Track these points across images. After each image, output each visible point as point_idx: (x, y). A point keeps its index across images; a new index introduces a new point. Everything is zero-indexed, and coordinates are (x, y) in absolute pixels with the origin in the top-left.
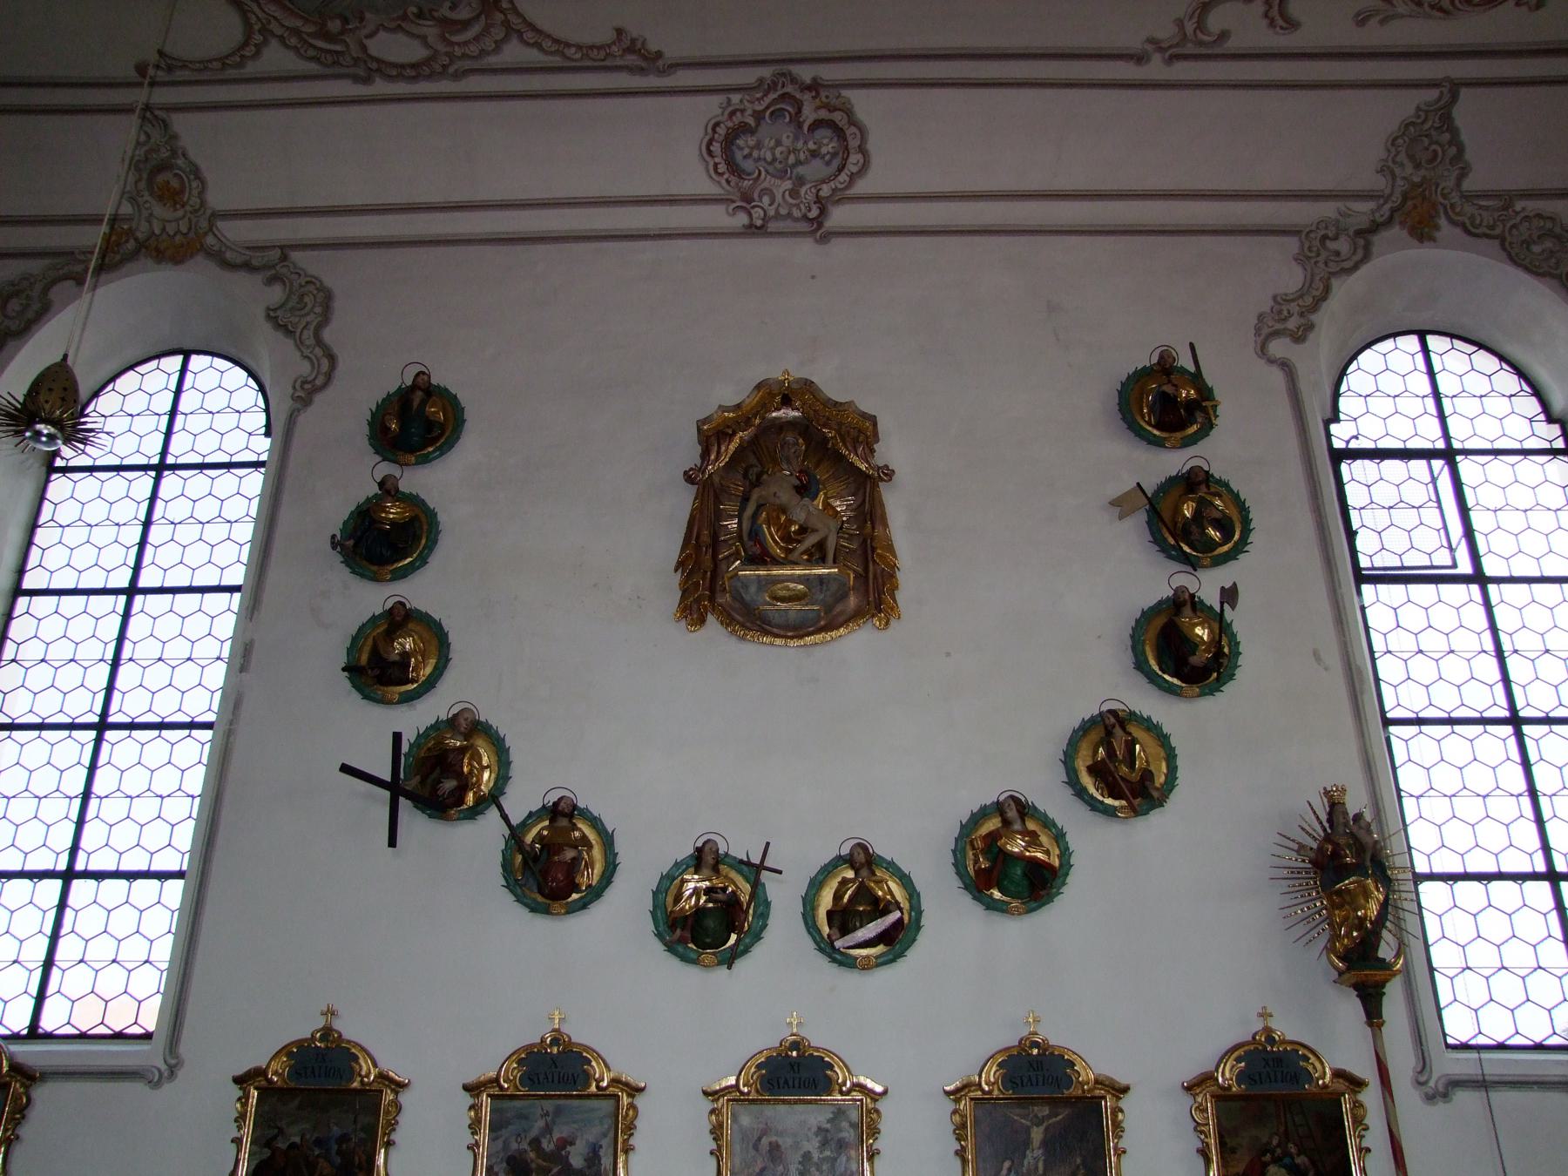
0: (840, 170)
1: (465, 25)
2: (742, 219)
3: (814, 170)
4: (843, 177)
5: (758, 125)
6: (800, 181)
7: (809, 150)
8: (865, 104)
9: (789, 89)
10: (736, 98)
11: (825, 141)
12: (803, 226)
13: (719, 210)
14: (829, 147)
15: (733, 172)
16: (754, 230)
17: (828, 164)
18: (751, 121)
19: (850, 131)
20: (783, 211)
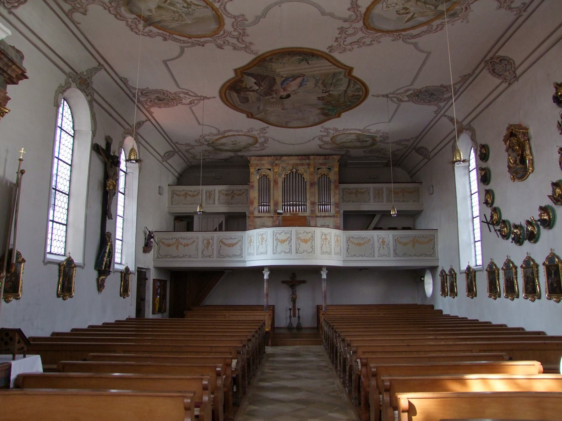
0: (511, 64)
2: (507, 83)
4: (513, 65)
6: (509, 70)
8: (501, 53)
9: (490, 61)
10: (486, 68)
12: (514, 79)
13: (503, 84)
14: (506, 62)
16: (510, 84)
17: (509, 65)
19: (505, 58)
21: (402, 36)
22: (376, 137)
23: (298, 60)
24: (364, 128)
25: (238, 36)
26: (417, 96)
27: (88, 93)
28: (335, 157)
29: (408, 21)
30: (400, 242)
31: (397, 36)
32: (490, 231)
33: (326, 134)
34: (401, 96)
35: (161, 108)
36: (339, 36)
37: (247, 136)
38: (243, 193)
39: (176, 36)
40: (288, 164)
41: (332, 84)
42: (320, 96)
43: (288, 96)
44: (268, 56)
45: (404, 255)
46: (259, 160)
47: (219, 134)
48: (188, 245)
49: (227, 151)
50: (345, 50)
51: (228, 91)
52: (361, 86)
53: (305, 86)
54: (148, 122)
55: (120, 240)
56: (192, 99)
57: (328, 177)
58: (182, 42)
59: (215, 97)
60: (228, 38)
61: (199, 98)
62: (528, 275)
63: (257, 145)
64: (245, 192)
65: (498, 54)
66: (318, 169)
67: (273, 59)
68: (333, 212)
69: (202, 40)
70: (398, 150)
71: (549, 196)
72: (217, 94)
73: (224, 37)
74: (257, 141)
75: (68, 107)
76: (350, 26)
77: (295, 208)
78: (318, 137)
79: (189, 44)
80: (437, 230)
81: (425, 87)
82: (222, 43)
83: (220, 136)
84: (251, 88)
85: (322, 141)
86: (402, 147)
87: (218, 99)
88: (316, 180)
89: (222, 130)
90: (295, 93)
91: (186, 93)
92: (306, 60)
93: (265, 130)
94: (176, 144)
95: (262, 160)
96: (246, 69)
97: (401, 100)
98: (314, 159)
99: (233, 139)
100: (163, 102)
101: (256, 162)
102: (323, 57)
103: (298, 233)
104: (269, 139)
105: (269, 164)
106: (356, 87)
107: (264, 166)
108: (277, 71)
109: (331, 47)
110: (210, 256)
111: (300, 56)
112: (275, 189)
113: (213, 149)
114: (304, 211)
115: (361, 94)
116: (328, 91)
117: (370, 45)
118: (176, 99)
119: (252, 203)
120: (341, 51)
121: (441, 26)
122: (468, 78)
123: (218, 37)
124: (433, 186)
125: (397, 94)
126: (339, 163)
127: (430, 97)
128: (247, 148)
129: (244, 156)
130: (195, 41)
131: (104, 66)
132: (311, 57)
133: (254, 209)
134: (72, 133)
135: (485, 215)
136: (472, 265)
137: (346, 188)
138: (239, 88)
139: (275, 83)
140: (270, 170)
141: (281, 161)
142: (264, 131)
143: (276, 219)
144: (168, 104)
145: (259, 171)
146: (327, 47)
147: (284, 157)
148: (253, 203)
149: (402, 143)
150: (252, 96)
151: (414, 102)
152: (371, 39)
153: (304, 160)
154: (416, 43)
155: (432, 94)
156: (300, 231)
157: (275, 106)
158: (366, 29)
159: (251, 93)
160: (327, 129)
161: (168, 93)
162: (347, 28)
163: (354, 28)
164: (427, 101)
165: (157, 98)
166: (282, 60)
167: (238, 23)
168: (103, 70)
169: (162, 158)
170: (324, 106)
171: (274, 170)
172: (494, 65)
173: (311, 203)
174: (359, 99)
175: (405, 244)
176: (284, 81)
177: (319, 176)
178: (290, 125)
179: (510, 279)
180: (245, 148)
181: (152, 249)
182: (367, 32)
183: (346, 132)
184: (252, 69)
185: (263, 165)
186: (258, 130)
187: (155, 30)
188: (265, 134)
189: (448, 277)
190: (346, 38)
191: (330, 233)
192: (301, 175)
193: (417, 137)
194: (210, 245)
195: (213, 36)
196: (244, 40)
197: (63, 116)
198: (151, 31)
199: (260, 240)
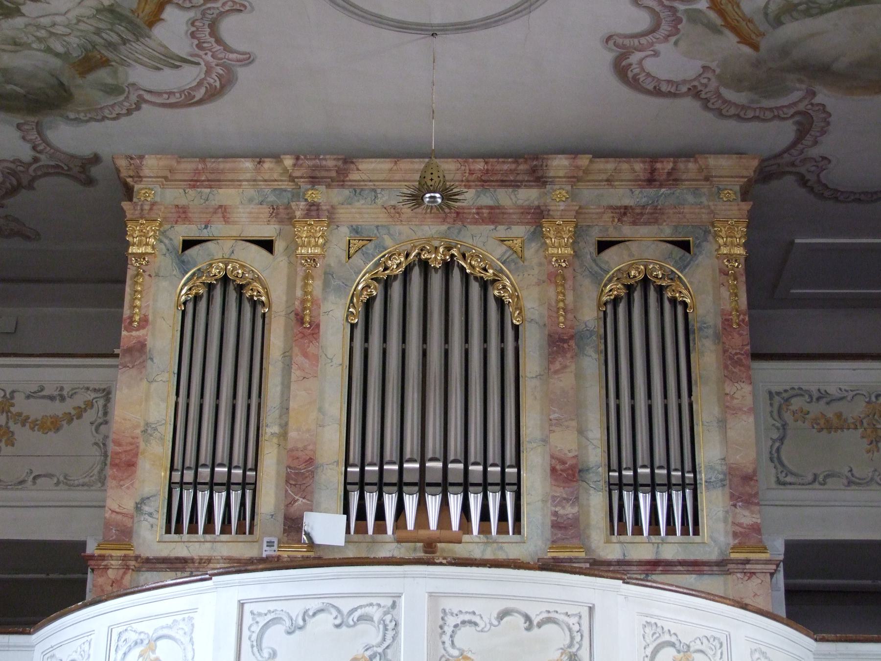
28: (721, 164)
38: (80, 412)
46: (194, 183)
57: (673, 301)
64: (90, 405)
66: (603, 246)
77: (433, 503)
88: (589, 315)
95: (215, 183)
98: (575, 179)
101: (173, 196)
103: (451, 621)
105: (266, 210)
107: (226, 220)
112: (296, 374)
114: (502, 530)
119: (128, 465)
126: (746, 206)
128: (105, 63)
129: (96, 159)
133: (138, 508)
137: (801, 392)
140: (267, 245)
141: (346, 192)
145: (193, 251)
148: (131, 465)
153: (504, 184)
156: (468, 605)
171: (293, 246)
173: (553, 470)
177: (616, 288)
185: (223, 212)
191: (723, 644)
192: (485, 285)
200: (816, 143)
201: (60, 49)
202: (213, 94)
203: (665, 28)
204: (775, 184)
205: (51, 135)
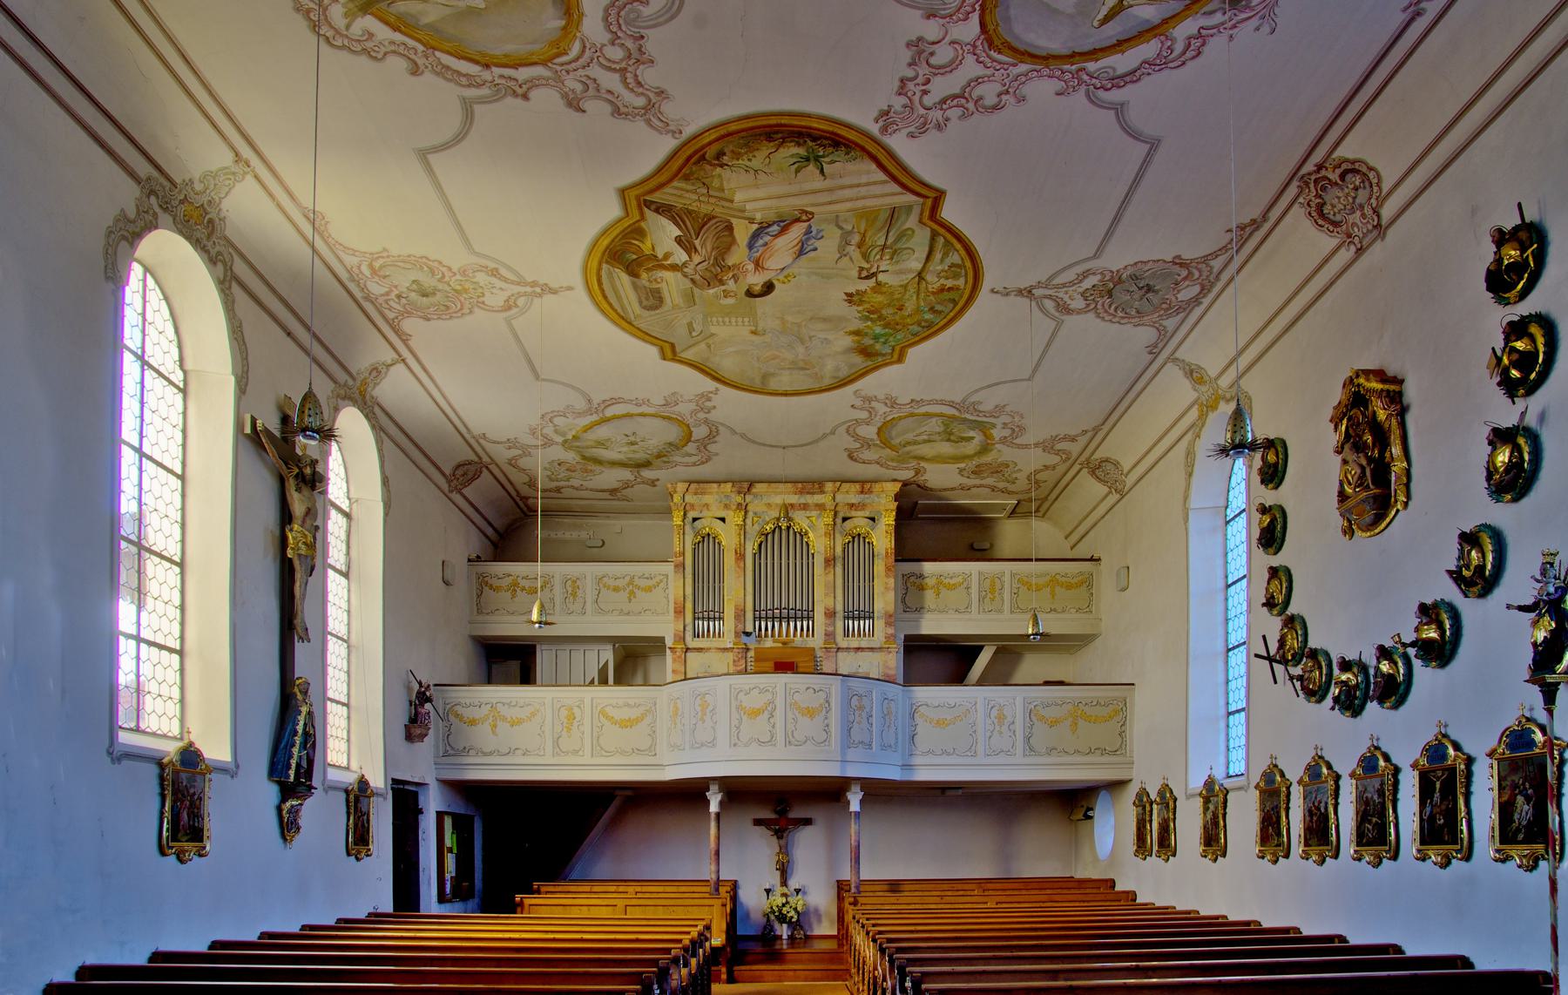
1: (1190, 273)
3: (1362, 196)
5: (1323, 199)
7: (1352, 189)
9: (1313, 177)
10: (1301, 200)
11: (1354, 179)
15: (1336, 227)
18: (1318, 200)
20: (1365, 231)
21: (1085, 77)
22: (994, 426)
23: (795, 160)
24: (964, 401)
25: (623, 65)
26: (1110, 293)
27: (213, 253)
29: (1107, 19)
30: (1042, 719)
31: (1073, 78)
32: (1276, 682)
33: (864, 415)
34: (1066, 293)
35: (429, 320)
36: (910, 73)
37: (664, 418)
39: (447, 60)
40: (769, 505)
41: (884, 247)
42: (852, 290)
43: (769, 288)
44: (710, 144)
45: (1051, 750)
47: (589, 412)
48: (520, 722)
49: (614, 464)
50: (923, 128)
51: (604, 266)
52: (962, 259)
53: (812, 254)
54: (401, 366)
55: (343, 704)
56: (508, 293)
58: (464, 81)
59: (570, 288)
60: (595, 71)
61: (528, 289)
62: (1370, 796)
63: (691, 448)
65: (1341, 152)
67: (724, 154)
68: (879, 638)
69: (523, 74)
70: (1046, 467)
71: (1450, 572)
72: (577, 280)
73: (584, 67)
74: (688, 438)
75: (162, 297)
76: (941, 37)
78: (846, 426)
79: (485, 91)
80: (1133, 684)
81: (1132, 263)
82: (579, 87)
83: (595, 418)
84: (667, 256)
85: (856, 437)
86: (1057, 459)
87: (581, 293)
89: (597, 399)
90: (786, 277)
91: (492, 270)
92: (817, 159)
93: (709, 400)
94: (482, 441)
95: (702, 493)
96: (651, 191)
97: (1064, 309)
99: (628, 426)
100: (431, 300)
102: (863, 149)
104: (721, 428)
106: (948, 261)
107: (708, 509)
108: (739, 197)
109: (887, 113)
110: (576, 752)
111: (799, 145)
113: (578, 458)
115: (962, 287)
116: (874, 275)
117: (996, 108)
118: (466, 291)
120: (912, 129)
121: (1198, 43)
122: (1251, 234)
123: (570, 63)
124: (1128, 568)
125: (1057, 287)
127: (1141, 299)
128: (665, 456)
129: (658, 480)
130: (502, 76)
131: (252, 164)
132: (831, 149)
134: (178, 377)
135: (1264, 637)
136: (1219, 774)
138: (635, 257)
139: (733, 242)
141: (751, 497)
142: (708, 404)
143: (740, 656)
144: (448, 308)
146: (875, 114)
147: (758, 486)
149: (1059, 446)
150: (671, 284)
151: (1098, 316)
152: (998, 88)
153: (808, 493)
154: (1122, 105)
155: (1149, 289)
157: (733, 320)
158: (986, 45)
159: (668, 275)
160: (869, 400)
161: (444, 269)
162: (934, 43)
163: (953, 42)
164: (1133, 312)
165: (414, 286)
166: (750, 160)
167: (623, 13)
168: (249, 178)
169: (449, 482)
170: (861, 325)
172: (1324, 189)
174: (955, 302)
175: (1053, 723)
176: (755, 236)
178: (773, 385)
179: (1318, 809)
180: (659, 456)
181: (431, 732)
182: (988, 56)
183: (916, 411)
184: (667, 190)
185: (707, 506)
186: (690, 401)
187: (383, 33)
188: (709, 412)
189: (1155, 806)
190: (928, 81)
193: (1096, 430)
194: (576, 724)
195: (551, 59)
196: (640, 79)
197: (144, 320)
198: (371, 35)
199: (699, 709)
200: (922, 476)
201: (649, 452)
202: (703, 463)
203: (865, 447)
204: (908, 487)
205: (642, 474)
